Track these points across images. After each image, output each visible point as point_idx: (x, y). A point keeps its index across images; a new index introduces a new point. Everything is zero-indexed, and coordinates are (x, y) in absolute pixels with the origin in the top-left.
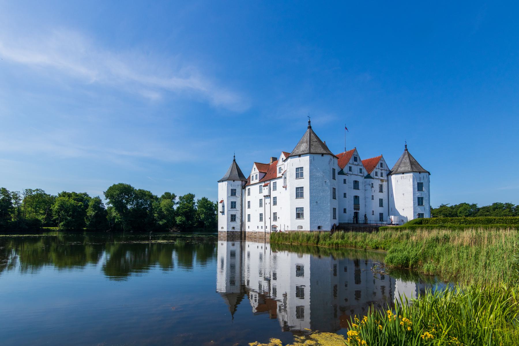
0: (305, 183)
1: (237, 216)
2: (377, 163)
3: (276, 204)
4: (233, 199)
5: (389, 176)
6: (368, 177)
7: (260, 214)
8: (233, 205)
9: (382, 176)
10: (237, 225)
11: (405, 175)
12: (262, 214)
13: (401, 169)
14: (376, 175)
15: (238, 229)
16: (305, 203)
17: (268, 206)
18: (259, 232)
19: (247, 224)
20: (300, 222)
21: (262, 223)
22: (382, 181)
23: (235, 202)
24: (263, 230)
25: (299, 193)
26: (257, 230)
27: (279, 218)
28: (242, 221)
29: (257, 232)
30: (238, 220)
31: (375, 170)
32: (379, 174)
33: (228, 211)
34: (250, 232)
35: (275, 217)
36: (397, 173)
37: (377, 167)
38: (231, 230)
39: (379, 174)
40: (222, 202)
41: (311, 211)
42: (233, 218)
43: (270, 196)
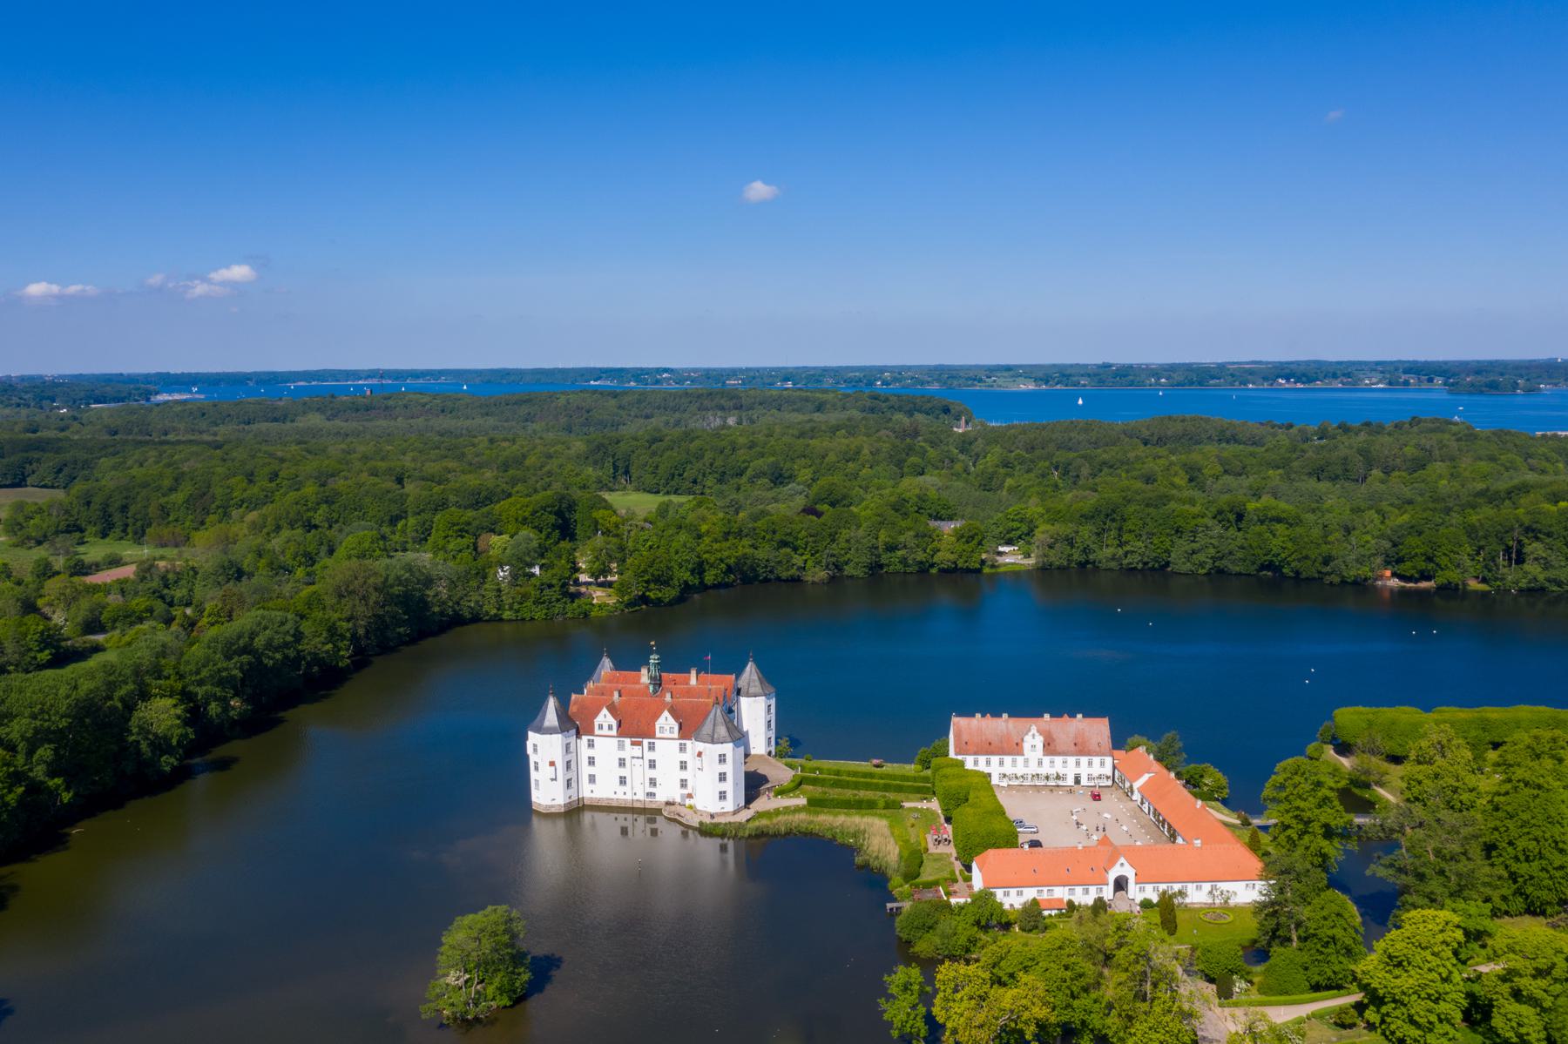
0: (728, 768)
4: (568, 757)
13: (752, 690)
15: (575, 798)
16: (728, 786)
20: (723, 804)
21: (627, 788)
24: (629, 797)
25: (722, 777)
30: (574, 784)
33: (564, 775)
35: (653, 782)
36: (748, 695)
38: (568, 801)
41: (734, 792)
42: (569, 783)
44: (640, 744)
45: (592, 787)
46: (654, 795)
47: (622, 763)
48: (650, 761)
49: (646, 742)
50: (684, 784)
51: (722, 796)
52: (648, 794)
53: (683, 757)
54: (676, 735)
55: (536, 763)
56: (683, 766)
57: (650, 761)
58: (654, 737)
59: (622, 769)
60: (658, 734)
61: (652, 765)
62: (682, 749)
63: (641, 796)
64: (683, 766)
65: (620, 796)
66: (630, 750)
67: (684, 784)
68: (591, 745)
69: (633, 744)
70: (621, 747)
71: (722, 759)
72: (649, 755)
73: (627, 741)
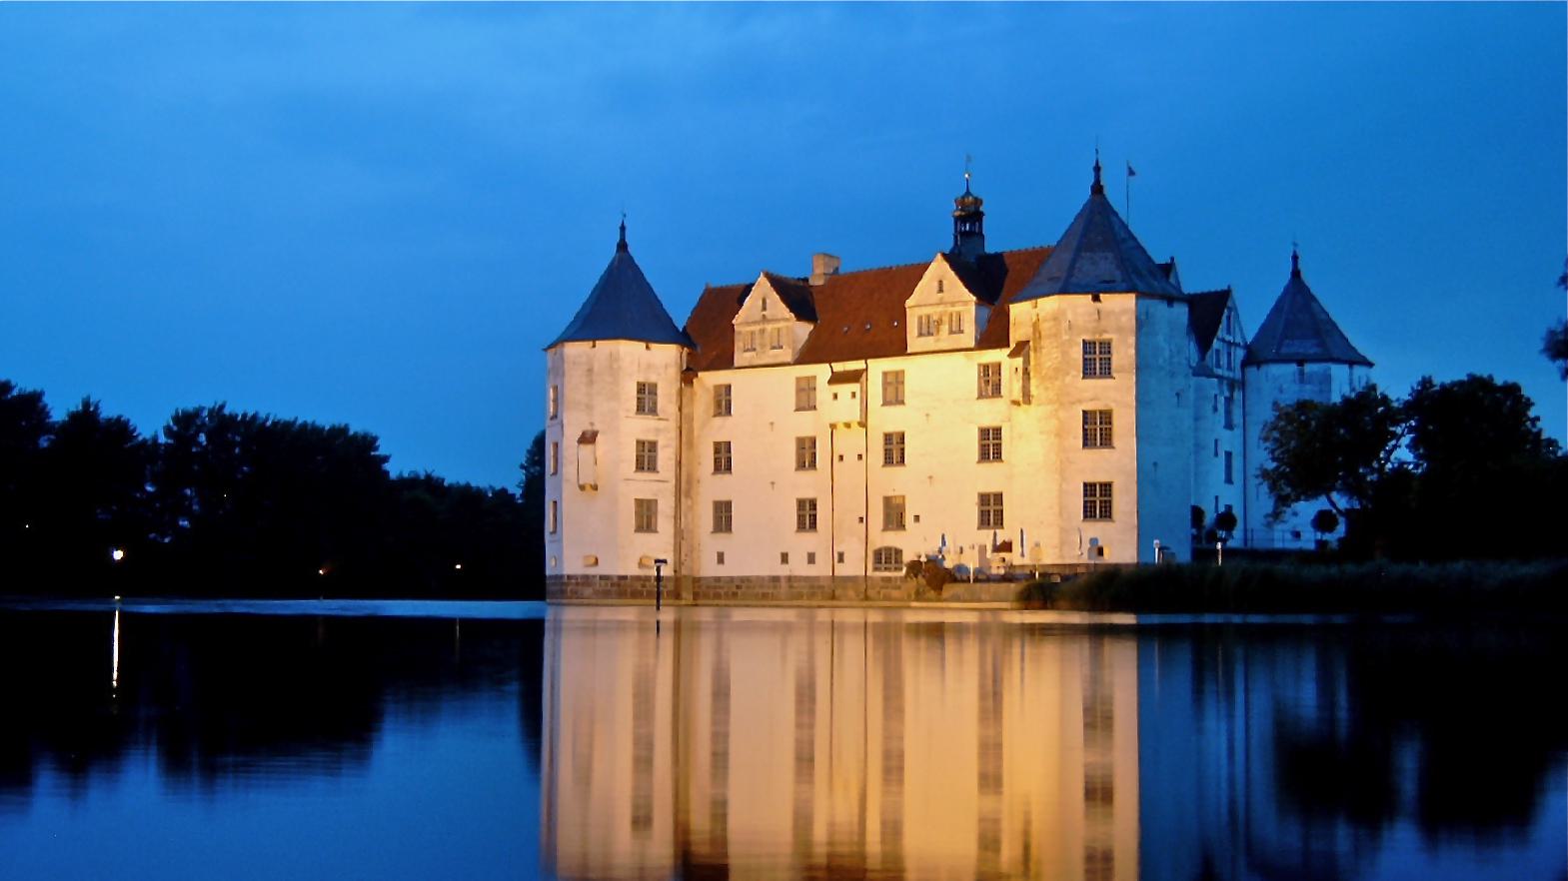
0: (1118, 394)
1: (660, 506)
2: (1219, 322)
3: (902, 461)
5: (1252, 371)
6: (1202, 371)
7: (801, 503)
8: (646, 455)
9: (1229, 368)
10: (659, 544)
11: (1309, 368)
12: (813, 504)
14: (1218, 366)
17: (849, 474)
18: (789, 579)
19: (708, 543)
22: (1232, 385)
23: (653, 445)
24: (821, 569)
25: (1097, 430)
26: (783, 571)
27: (917, 518)
28: (679, 535)
29: (775, 579)
31: (1216, 344)
32: (1224, 361)
34: (732, 579)
35: (895, 515)
37: (1220, 334)
39: (1224, 361)
40: (588, 438)
42: (646, 517)
43: (863, 424)
44: (855, 377)
45: (722, 542)
46: (899, 552)
47: (806, 455)
48: (888, 438)
49: (878, 367)
50: (991, 510)
51: (1097, 501)
52: (878, 554)
53: (991, 413)
54: (969, 337)
55: (556, 445)
56: (991, 445)
57: (888, 438)
58: (899, 348)
59: (807, 476)
60: (914, 342)
61: (894, 449)
62: (990, 383)
63: (853, 567)
64: (991, 445)
65: (799, 567)
66: (838, 404)
67: (991, 510)
68: (723, 403)
69: (837, 379)
70: (806, 398)
71: (1096, 360)
72: (886, 419)
73: (822, 372)
